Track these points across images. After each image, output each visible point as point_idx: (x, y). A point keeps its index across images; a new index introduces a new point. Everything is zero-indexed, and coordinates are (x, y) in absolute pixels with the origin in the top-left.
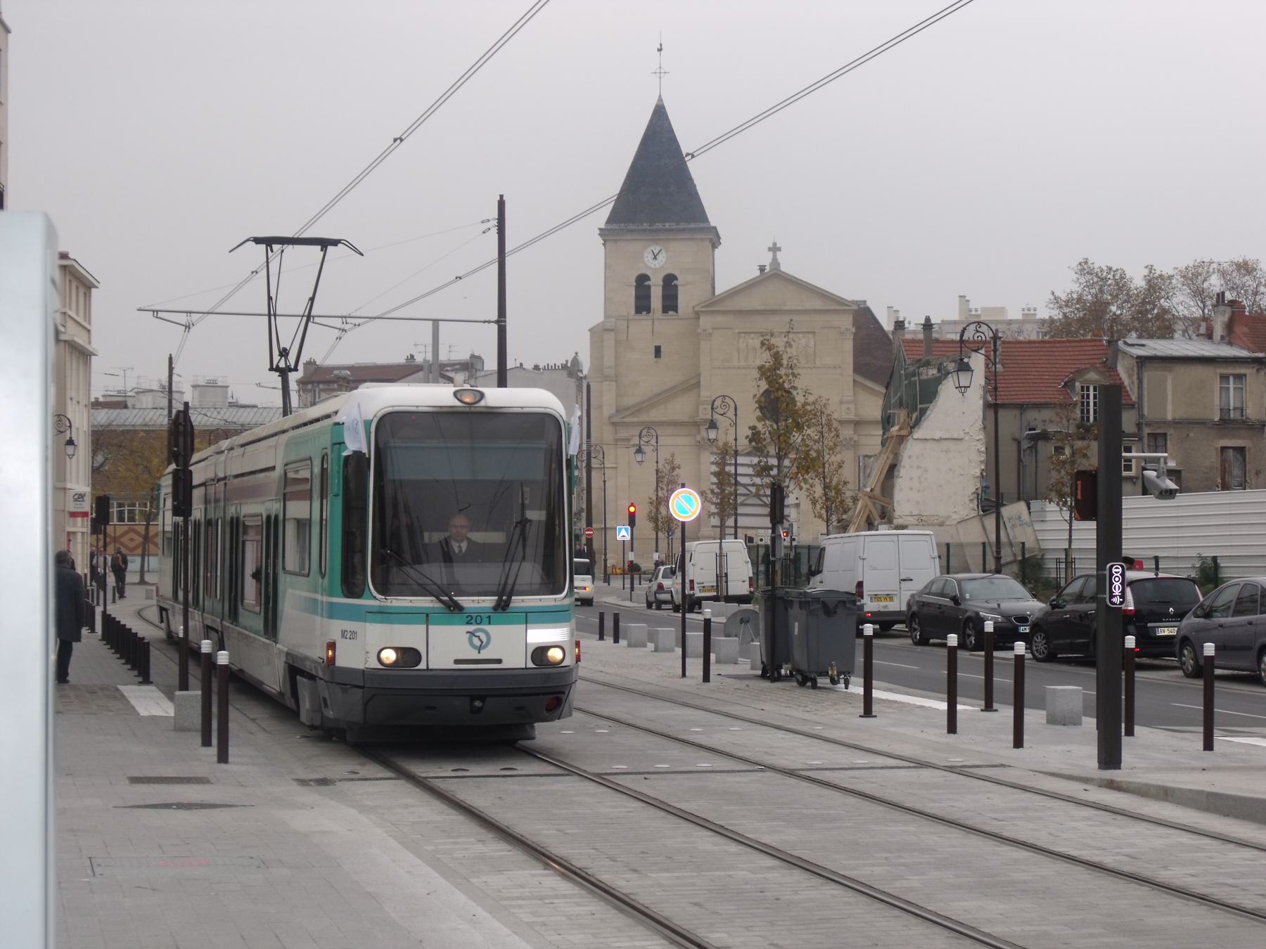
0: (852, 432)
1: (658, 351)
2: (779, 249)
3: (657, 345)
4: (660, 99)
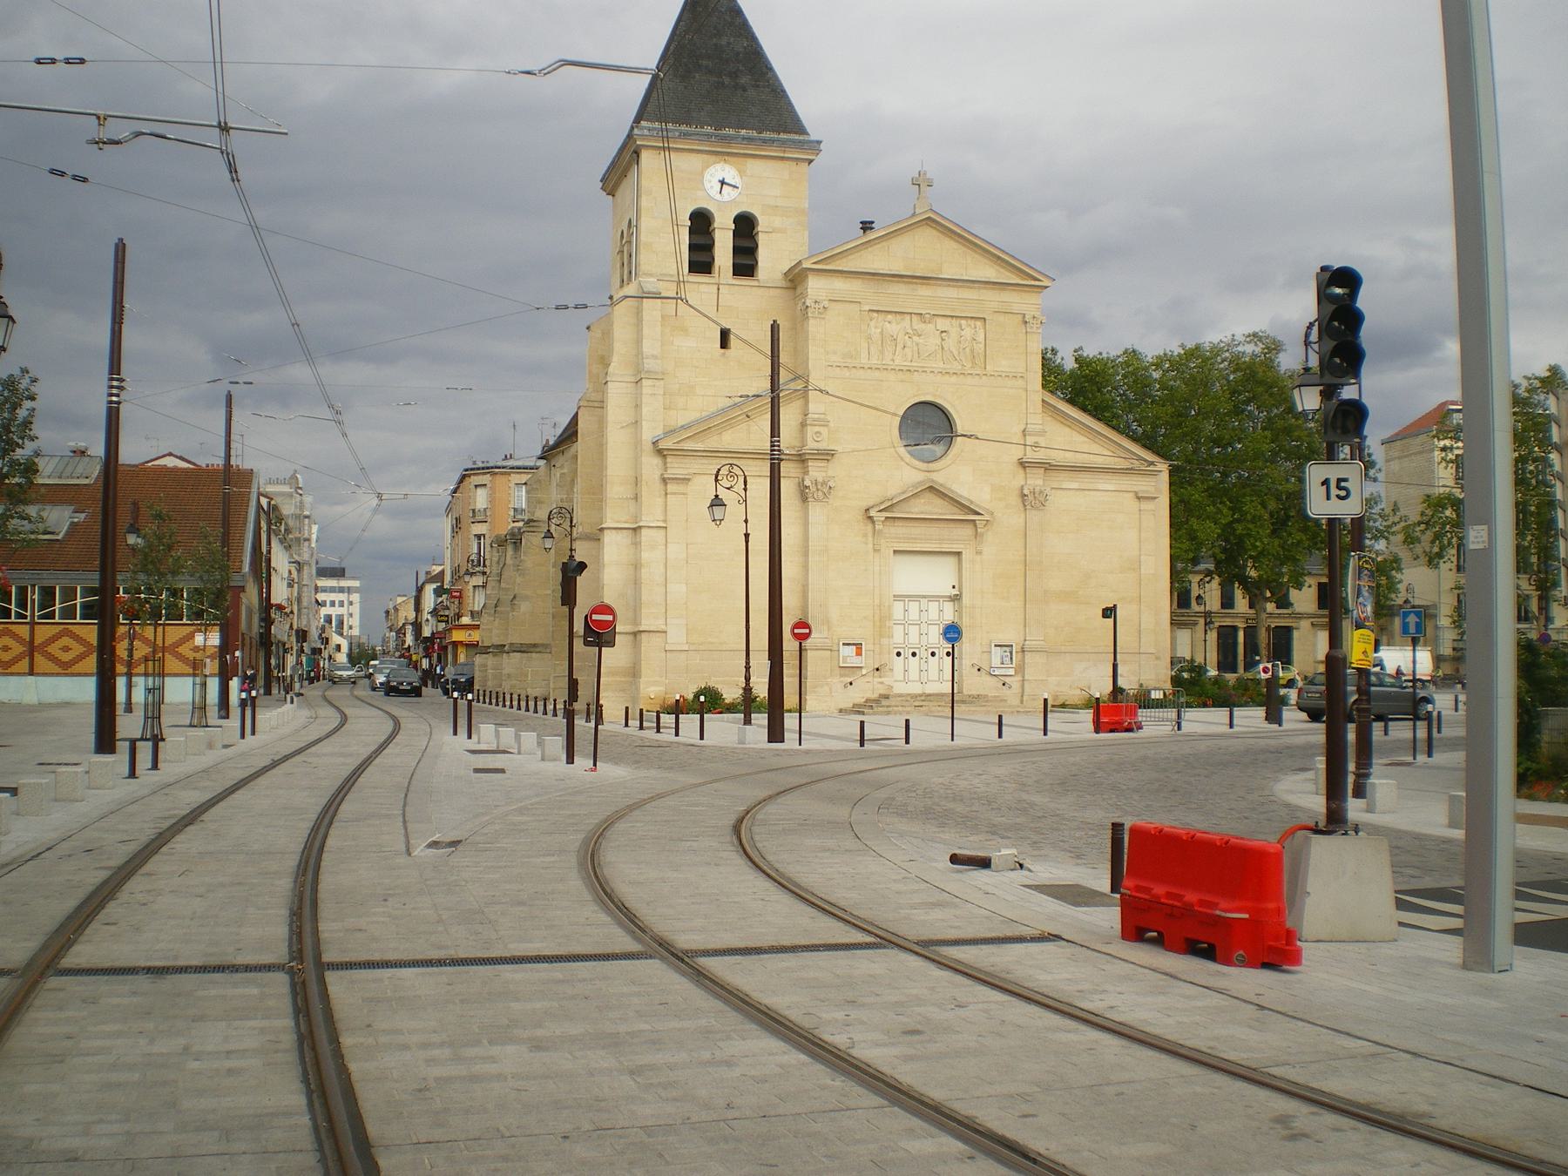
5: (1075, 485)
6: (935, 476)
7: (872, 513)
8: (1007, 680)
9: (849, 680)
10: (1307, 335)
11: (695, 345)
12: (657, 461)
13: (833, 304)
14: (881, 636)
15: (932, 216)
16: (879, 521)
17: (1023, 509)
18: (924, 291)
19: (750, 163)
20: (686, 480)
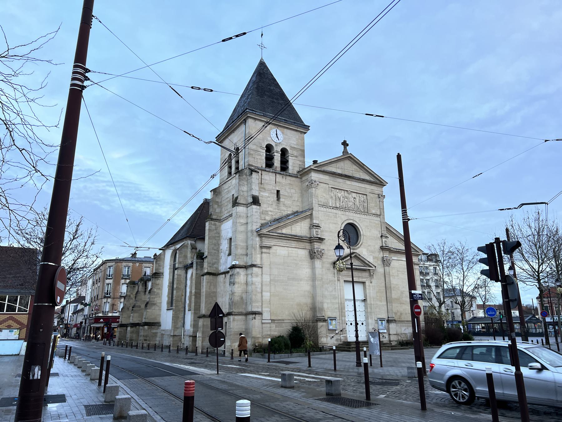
2: (348, 145)
4: (262, 59)
5: (396, 258)
8: (384, 335)
9: (332, 335)
10: (338, 235)
12: (258, 239)
13: (320, 183)
14: (342, 316)
17: (383, 266)
18: (348, 182)
19: (285, 130)
20: (269, 248)
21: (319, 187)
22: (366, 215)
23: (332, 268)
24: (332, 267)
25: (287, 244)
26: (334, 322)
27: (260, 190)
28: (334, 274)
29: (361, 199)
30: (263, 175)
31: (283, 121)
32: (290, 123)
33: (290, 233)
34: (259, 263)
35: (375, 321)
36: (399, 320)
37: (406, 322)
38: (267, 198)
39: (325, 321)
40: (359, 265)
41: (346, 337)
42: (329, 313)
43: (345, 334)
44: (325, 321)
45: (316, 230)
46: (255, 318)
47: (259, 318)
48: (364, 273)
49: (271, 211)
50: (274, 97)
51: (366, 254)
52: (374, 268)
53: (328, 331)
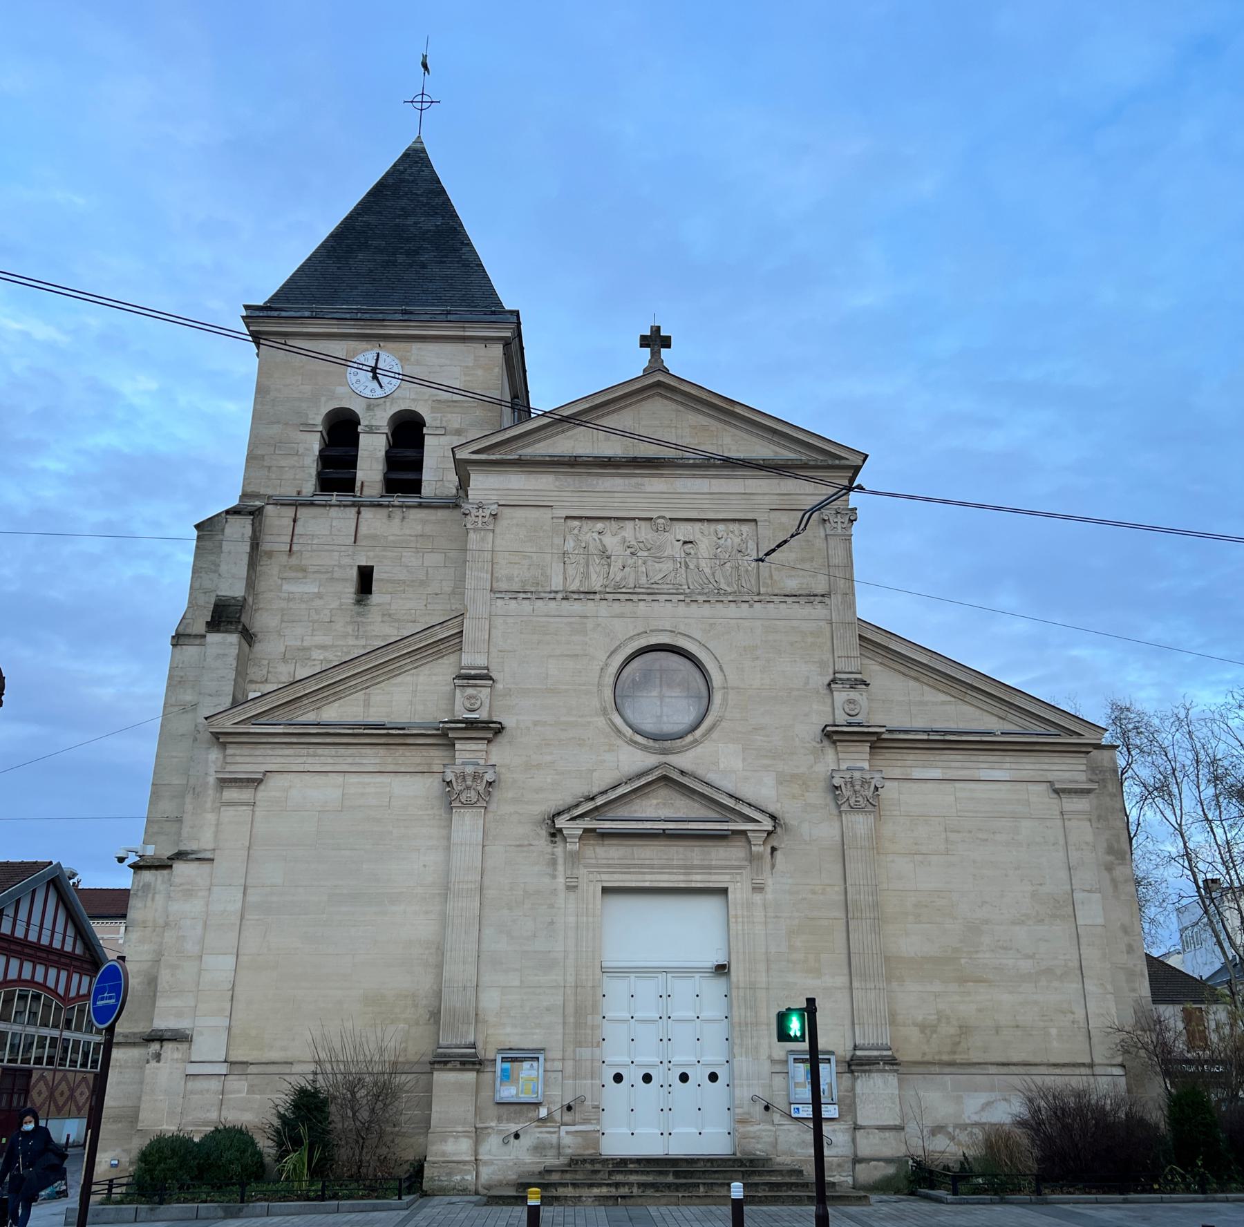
0: (866, 765)
1: (365, 579)
2: (666, 342)
3: (363, 563)
4: (419, 141)
6: (673, 759)
7: (561, 823)
9: (514, 1128)
11: (316, 590)
15: (662, 379)
16: (572, 836)
17: (835, 812)
18: (656, 485)
19: (415, 347)
20: (255, 782)
21: (503, 523)
22: (746, 605)
23: (542, 842)
24: (544, 833)
25: (340, 760)
26: (527, 1071)
27: (285, 575)
28: (553, 862)
29: (722, 541)
30: (299, 523)
31: (399, 317)
32: (427, 317)
33: (360, 719)
34: (210, 846)
35: (773, 1062)
36: (945, 1058)
37: (992, 1069)
38: (312, 600)
39: (472, 1062)
40: (693, 815)
41: (593, 1138)
42: (508, 1030)
43: (586, 1121)
44: (472, 1062)
45: (470, 691)
46: (158, 1057)
47: (177, 1055)
48: (721, 850)
49: (323, 647)
50: (402, 248)
51: (738, 764)
52: (768, 825)
53: (493, 1111)
